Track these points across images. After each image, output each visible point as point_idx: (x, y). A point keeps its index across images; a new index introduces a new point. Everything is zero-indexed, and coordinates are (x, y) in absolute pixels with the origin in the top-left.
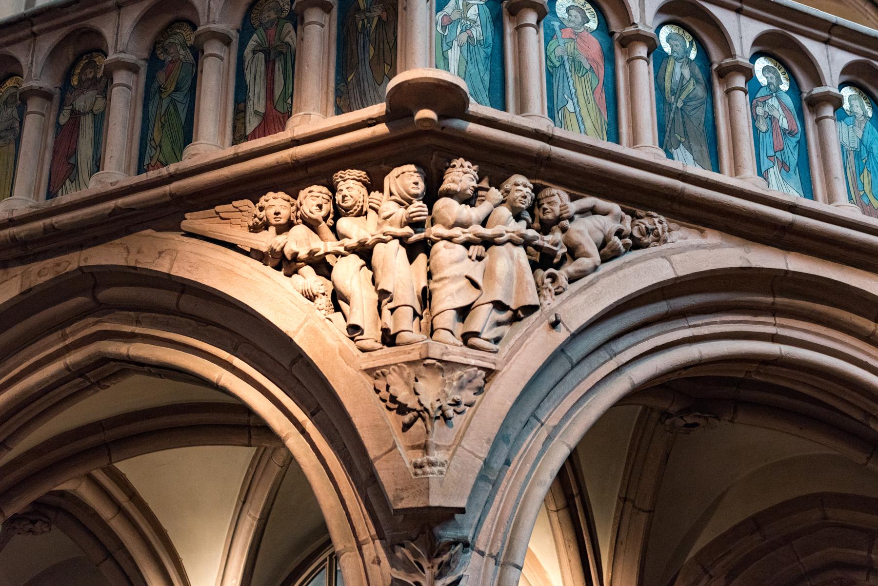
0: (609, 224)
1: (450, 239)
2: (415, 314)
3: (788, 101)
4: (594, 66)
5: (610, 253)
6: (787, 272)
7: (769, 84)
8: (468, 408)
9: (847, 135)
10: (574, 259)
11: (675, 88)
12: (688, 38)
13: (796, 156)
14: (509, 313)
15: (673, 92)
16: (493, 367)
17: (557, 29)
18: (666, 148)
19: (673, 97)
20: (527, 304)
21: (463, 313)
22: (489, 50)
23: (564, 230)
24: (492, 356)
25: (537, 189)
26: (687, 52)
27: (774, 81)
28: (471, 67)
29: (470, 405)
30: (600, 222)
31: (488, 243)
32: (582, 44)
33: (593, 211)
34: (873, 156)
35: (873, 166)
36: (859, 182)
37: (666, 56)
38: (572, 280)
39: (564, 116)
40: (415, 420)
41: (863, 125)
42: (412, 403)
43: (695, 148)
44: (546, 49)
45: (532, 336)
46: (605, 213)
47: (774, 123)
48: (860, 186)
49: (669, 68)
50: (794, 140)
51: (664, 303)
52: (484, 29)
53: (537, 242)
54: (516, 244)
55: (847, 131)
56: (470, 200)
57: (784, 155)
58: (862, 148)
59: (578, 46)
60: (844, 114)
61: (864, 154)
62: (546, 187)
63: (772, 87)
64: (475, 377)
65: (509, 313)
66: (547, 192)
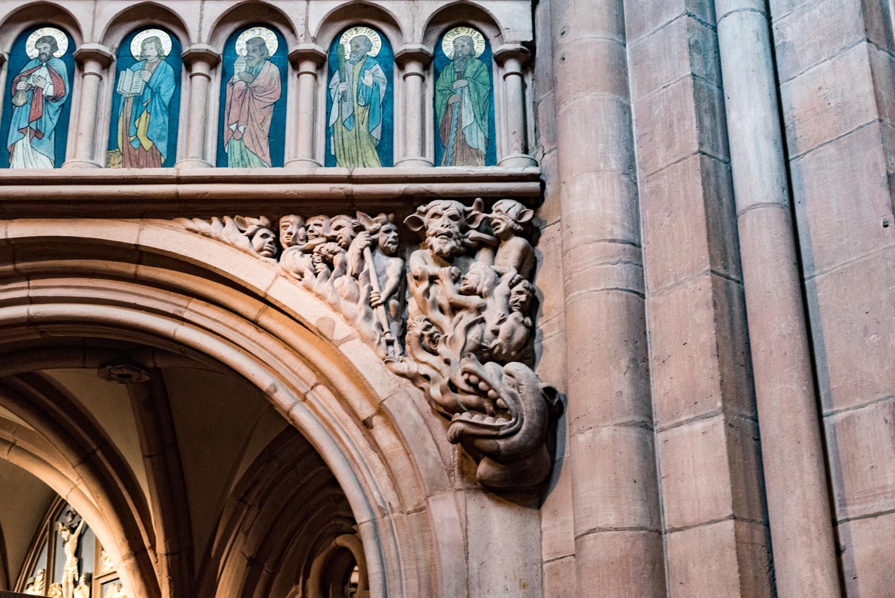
3: (61, 67)
7: (40, 55)
9: (130, 83)
13: (55, 121)
27: (47, 51)
34: (159, 96)
35: (155, 107)
36: (132, 127)
47: (36, 94)
48: (132, 133)
50: (57, 105)
55: (131, 79)
58: (147, 91)
60: (132, 60)
61: (148, 96)
63: (44, 57)
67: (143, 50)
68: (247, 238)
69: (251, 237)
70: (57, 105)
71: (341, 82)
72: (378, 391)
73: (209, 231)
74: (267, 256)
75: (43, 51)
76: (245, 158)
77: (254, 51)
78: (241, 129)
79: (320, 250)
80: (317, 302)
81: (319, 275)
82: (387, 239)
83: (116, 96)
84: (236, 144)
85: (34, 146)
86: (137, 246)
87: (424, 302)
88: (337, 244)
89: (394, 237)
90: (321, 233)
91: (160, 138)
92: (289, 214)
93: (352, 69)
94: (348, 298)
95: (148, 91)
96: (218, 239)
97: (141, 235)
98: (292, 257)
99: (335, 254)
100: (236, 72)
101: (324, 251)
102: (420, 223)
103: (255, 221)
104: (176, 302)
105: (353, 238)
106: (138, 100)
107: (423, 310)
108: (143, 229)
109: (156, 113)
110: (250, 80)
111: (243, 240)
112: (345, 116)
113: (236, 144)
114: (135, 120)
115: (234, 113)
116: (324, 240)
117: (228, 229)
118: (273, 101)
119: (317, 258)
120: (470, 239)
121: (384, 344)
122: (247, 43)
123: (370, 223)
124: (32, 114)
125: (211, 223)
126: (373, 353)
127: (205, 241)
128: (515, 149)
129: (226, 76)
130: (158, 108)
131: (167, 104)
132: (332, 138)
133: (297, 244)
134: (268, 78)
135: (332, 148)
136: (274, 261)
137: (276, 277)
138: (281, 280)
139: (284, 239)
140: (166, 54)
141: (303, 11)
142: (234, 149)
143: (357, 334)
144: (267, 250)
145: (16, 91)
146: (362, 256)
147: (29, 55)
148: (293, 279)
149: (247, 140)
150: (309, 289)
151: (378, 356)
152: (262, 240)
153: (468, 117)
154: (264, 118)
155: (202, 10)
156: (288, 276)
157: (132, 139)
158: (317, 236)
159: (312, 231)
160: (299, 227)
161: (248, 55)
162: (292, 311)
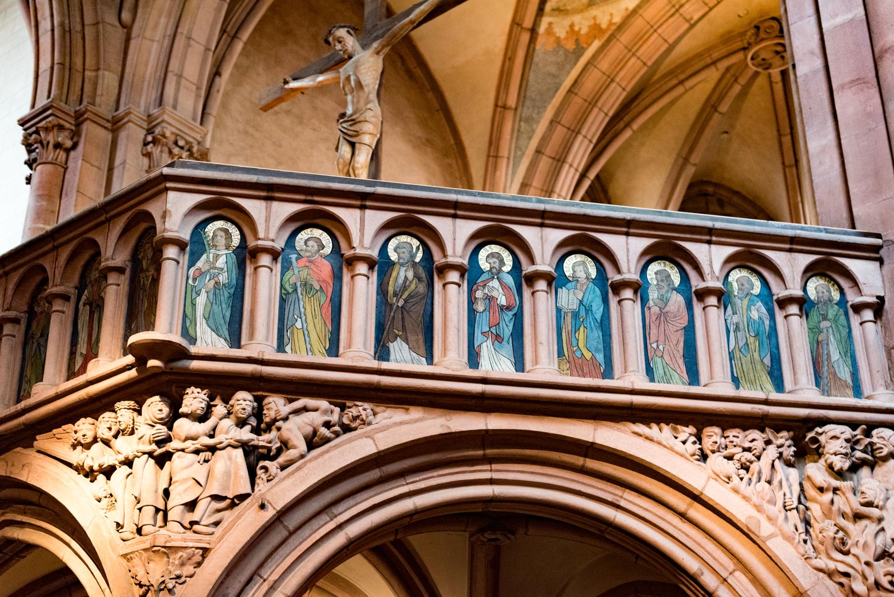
0: (317, 419)
1: (183, 450)
2: (157, 510)
3: (509, 280)
5: (319, 441)
6: (487, 431)
7: (491, 268)
8: (188, 579)
10: (288, 449)
11: (398, 290)
12: (415, 243)
13: (511, 328)
14: (228, 501)
15: (395, 294)
16: (208, 546)
17: (294, 260)
19: (395, 298)
20: (239, 493)
21: (191, 506)
22: (232, 291)
23: (279, 429)
24: (208, 538)
25: (259, 400)
26: (413, 256)
27: (497, 265)
28: (215, 307)
29: (191, 576)
30: (309, 419)
31: (213, 449)
32: (315, 269)
33: (305, 409)
35: (590, 322)
37: (393, 264)
38: (283, 468)
39: (292, 333)
40: (147, 591)
41: (585, 287)
42: (144, 581)
43: (411, 338)
44: (282, 280)
45: (243, 518)
46: (316, 410)
48: (574, 343)
49: (394, 274)
50: (511, 314)
51: (377, 470)
52: (230, 273)
53: (252, 443)
54: (235, 447)
56: (202, 418)
57: (499, 328)
61: (583, 313)
62: (266, 397)
63: (494, 270)
64: (194, 555)
66: (266, 401)
67: (574, 271)
69: (684, 442)
70: (511, 314)
71: (733, 314)
72: (802, 583)
75: (493, 265)
76: (668, 373)
77: (662, 281)
78: (661, 347)
80: (743, 503)
82: (789, 452)
83: (559, 310)
84: (659, 360)
85: (497, 349)
87: (830, 510)
89: (794, 451)
90: (739, 444)
91: (597, 350)
93: (741, 304)
94: (769, 502)
95: (582, 309)
98: (716, 461)
99: (751, 462)
100: (651, 298)
101: (743, 460)
102: (815, 440)
103: (685, 429)
105: (764, 449)
106: (576, 315)
107: (827, 514)
109: (591, 328)
110: (663, 306)
112: (741, 344)
113: (659, 360)
114: (575, 333)
115: (654, 331)
116: (741, 450)
117: (664, 433)
118: (683, 326)
120: (856, 458)
121: (802, 543)
122: (656, 273)
123: (777, 438)
124: (491, 320)
126: (793, 550)
127: (648, 443)
128: (881, 385)
129: (644, 301)
130: (592, 323)
131: (599, 321)
132: (733, 362)
133: (719, 451)
134: (677, 306)
135: (735, 370)
137: (708, 479)
138: (712, 482)
140: (593, 277)
141: (707, 253)
142: (658, 365)
143: (779, 533)
145: (476, 298)
146: (773, 466)
147: (482, 267)
148: (722, 481)
149: (666, 357)
150: (736, 491)
151: (798, 552)
153: (835, 356)
154: (678, 340)
155: (627, 244)
156: (718, 478)
157: (575, 349)
158: (735, 446)
159: (732, 442)
161: (658, 284)
162: (724, 508)
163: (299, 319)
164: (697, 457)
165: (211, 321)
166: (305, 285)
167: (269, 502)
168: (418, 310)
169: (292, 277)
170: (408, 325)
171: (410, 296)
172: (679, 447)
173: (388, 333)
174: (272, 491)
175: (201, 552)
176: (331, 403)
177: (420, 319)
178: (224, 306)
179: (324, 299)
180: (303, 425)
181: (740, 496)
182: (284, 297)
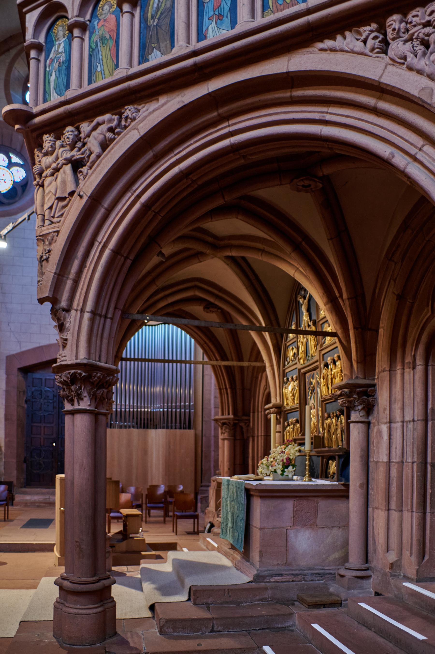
4: (111, 33)
6: (209, 94)
11: (154, 13)
15: (153, 17)
18: (146, 58)
19: (152, 20)
33: (98, 124)
38: (91, 168)
43: (162, 45)
46: (103, 123)
53: (74, 158)
57: (221, 8)
59: (105, 28)
62: (79, 125)
65: (68, 199)
68: (362, 44)
69: (365, 42)
73: (334, 46)
74: (378, 53)
79: (418, 36)
81: (418, 55)
86: (287, 73)
88: (431, 28)
92: (391, 15)
96: (342, 51)
97: (290, 64)
101: (421, 35)
104: (320, 110)
108: (290, 59)
111: (359, 46)
116: (421, 26)
119: (416, 43)
125: (335, 40)
127: (332, 55)
133: (400, 37)
136: (383, 55)
139: (390, 36)
144: (378, 48)
152: (373, 42)
158: (415, 26)
159: (411, 22)
160: (401, 22)
163: (99, 65)
164: (377, 50)
165: (58, 89)
166: (102, 39)
167: (84, 193)
168: (168, 20)
169: (95, 38)
170: (160, 36)
171: (162, 14)
172: (359, 46)
173: (148, 49)
174: (86, 185)
175: (56, 234)
176: (113, 115)
177: (167, 28)
178: (63, 76)
179: (111, 43)
180: (97, 135)
181: (414, 73)
182: (91, 53)
